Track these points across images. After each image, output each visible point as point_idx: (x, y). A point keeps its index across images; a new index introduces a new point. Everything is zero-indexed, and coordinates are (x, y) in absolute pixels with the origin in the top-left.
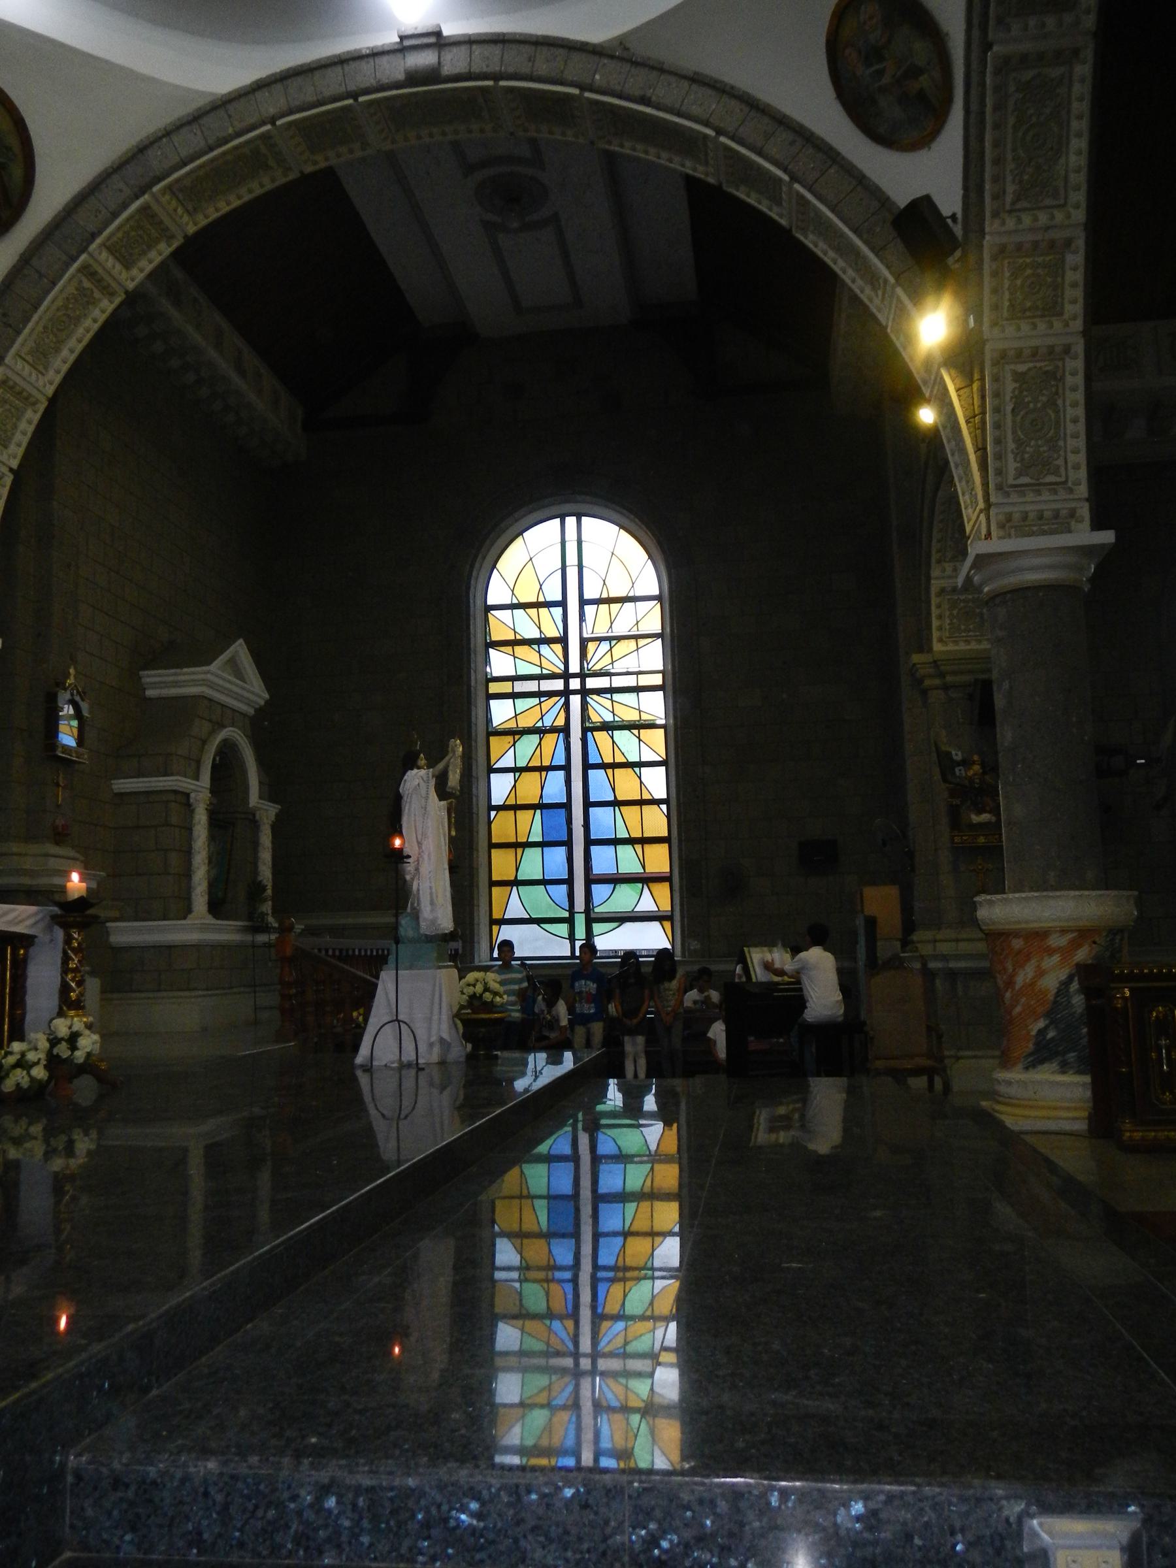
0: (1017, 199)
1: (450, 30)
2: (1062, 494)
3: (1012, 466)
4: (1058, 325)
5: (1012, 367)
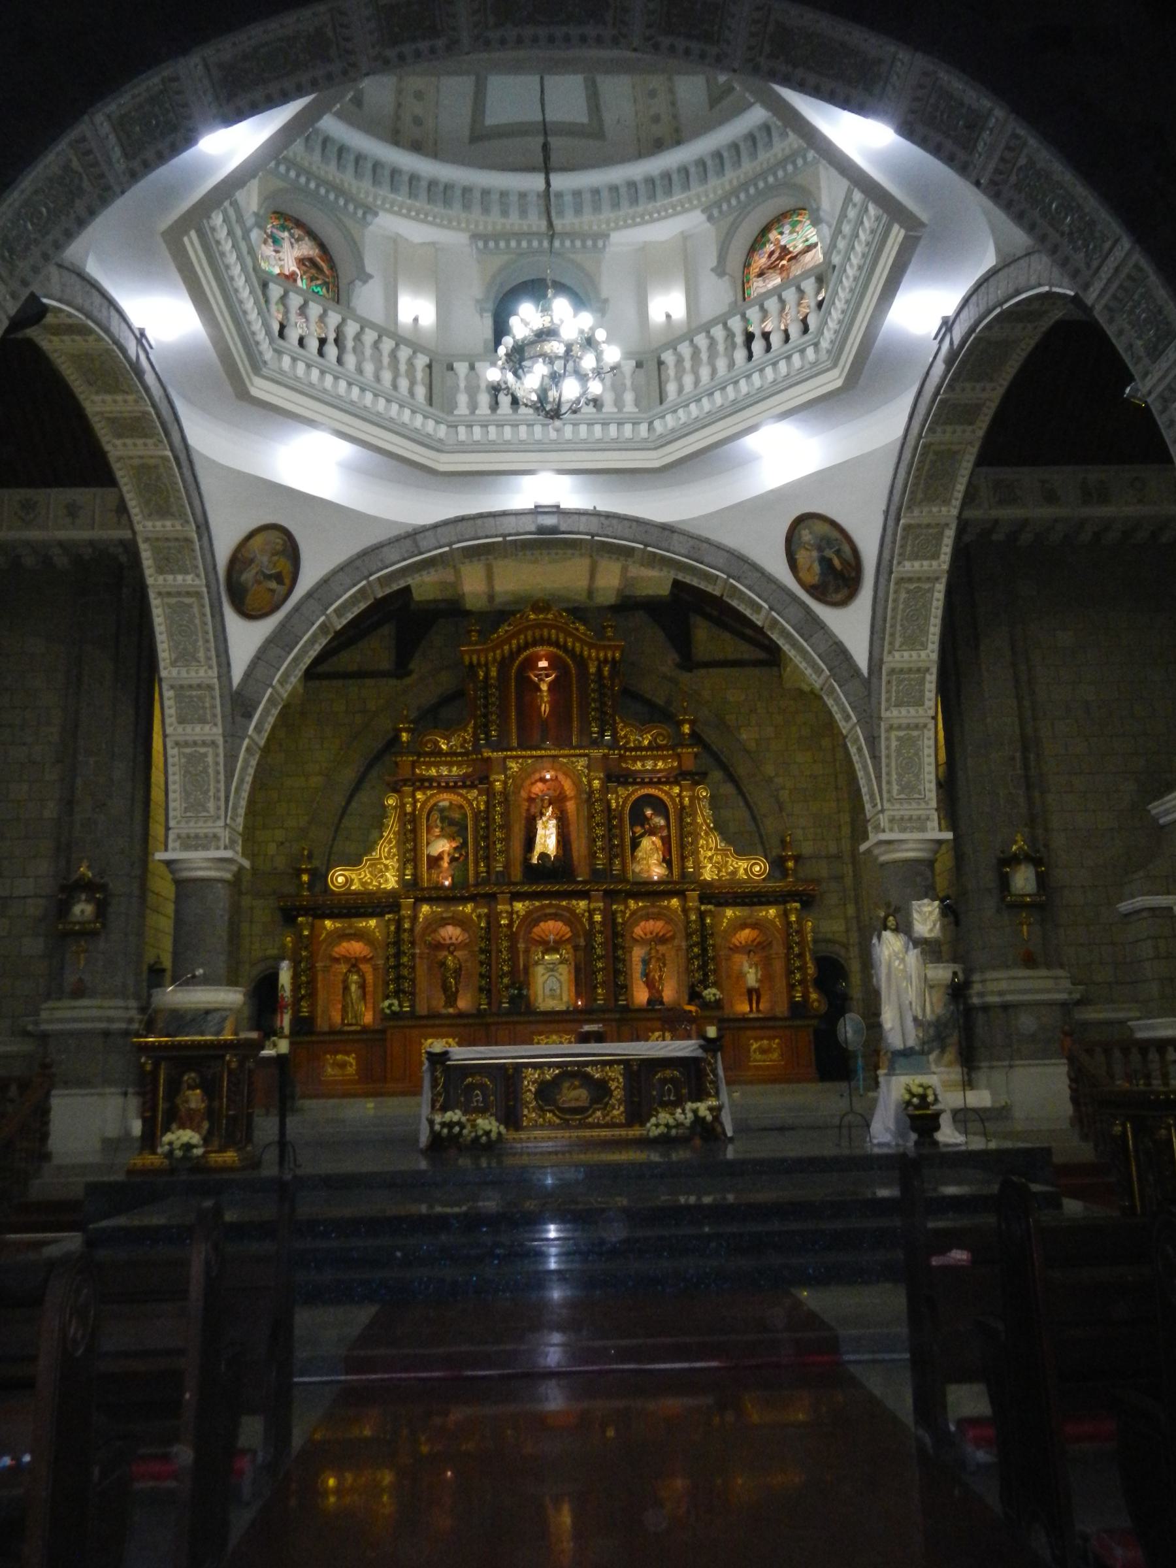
0: (900, 646)
1: (565, 505)
2: (923, 806)
3: (895, 788)
4: (920, 709)
5: (896, 733)
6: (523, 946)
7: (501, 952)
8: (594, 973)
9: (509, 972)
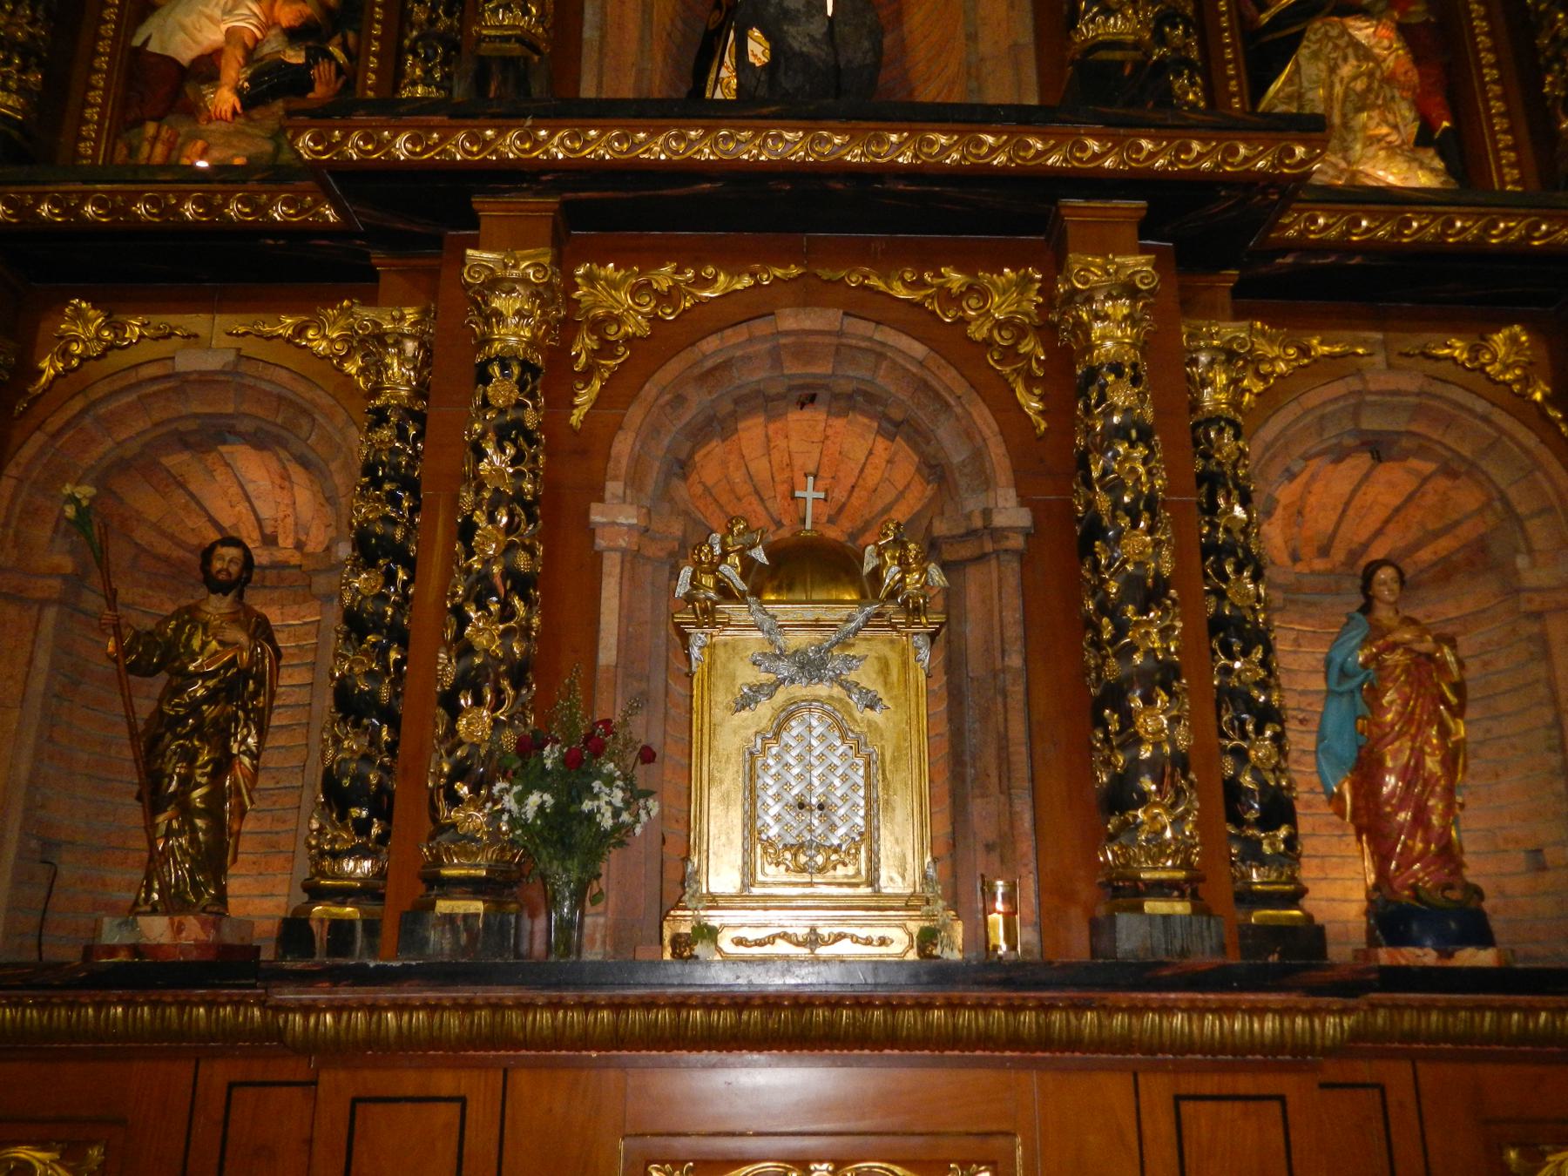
6: (628, 517)
7: (467, 530)
8: (1115, 696)
9: (519, 673)
